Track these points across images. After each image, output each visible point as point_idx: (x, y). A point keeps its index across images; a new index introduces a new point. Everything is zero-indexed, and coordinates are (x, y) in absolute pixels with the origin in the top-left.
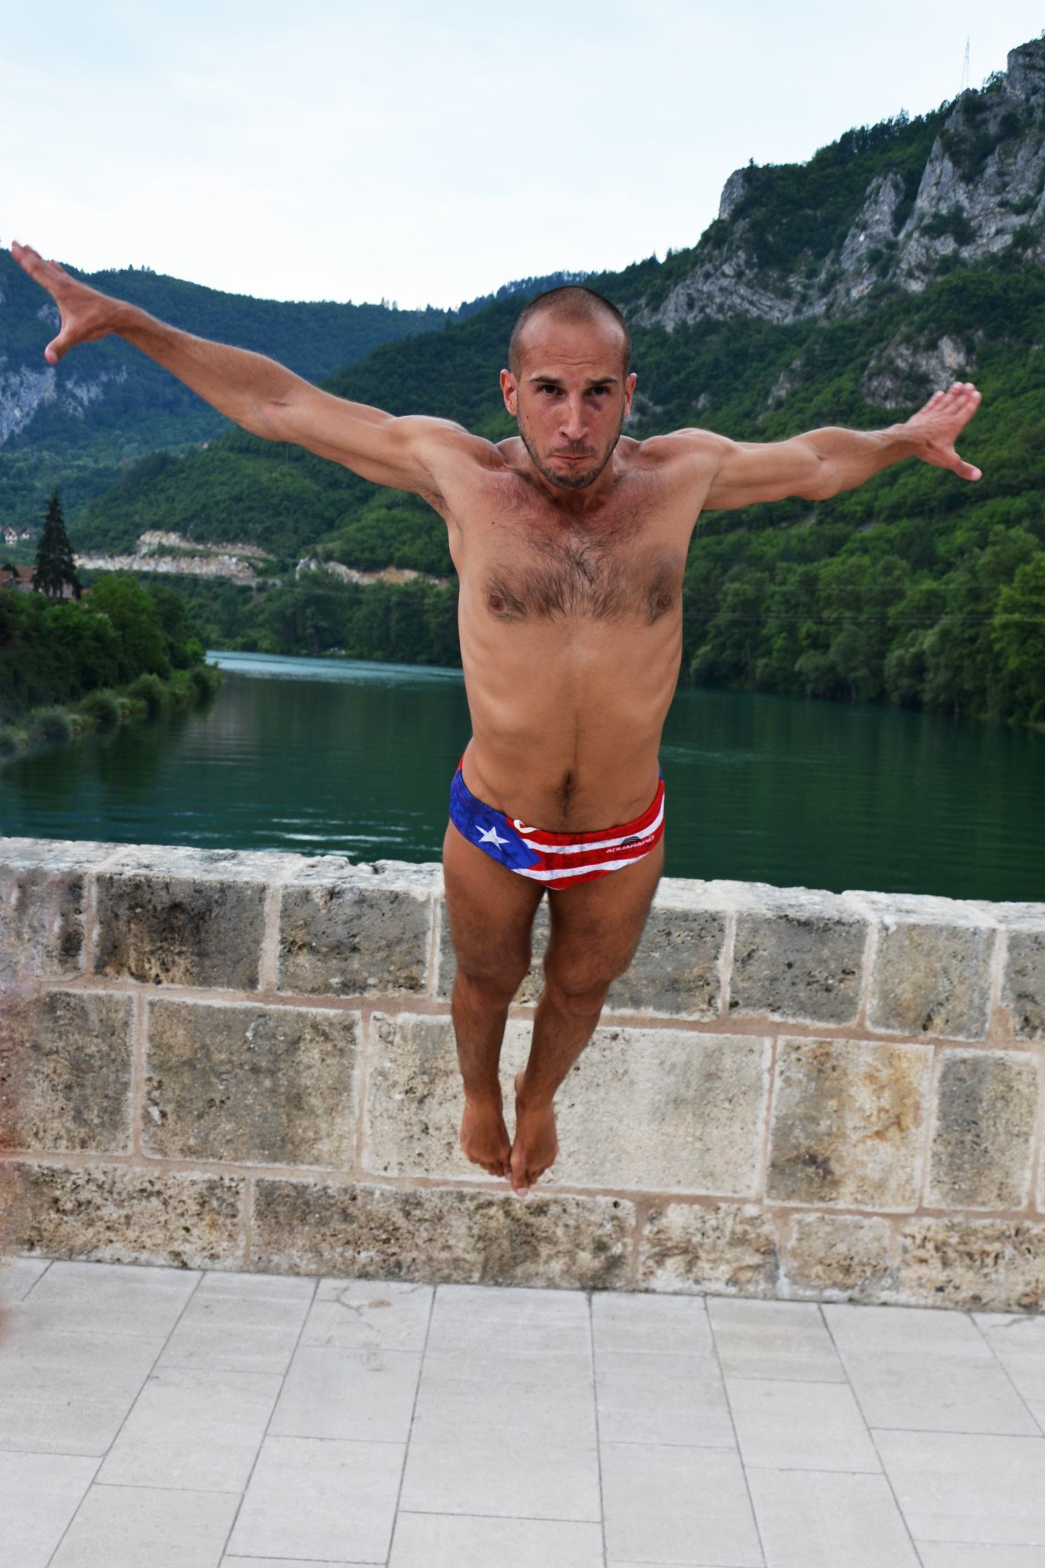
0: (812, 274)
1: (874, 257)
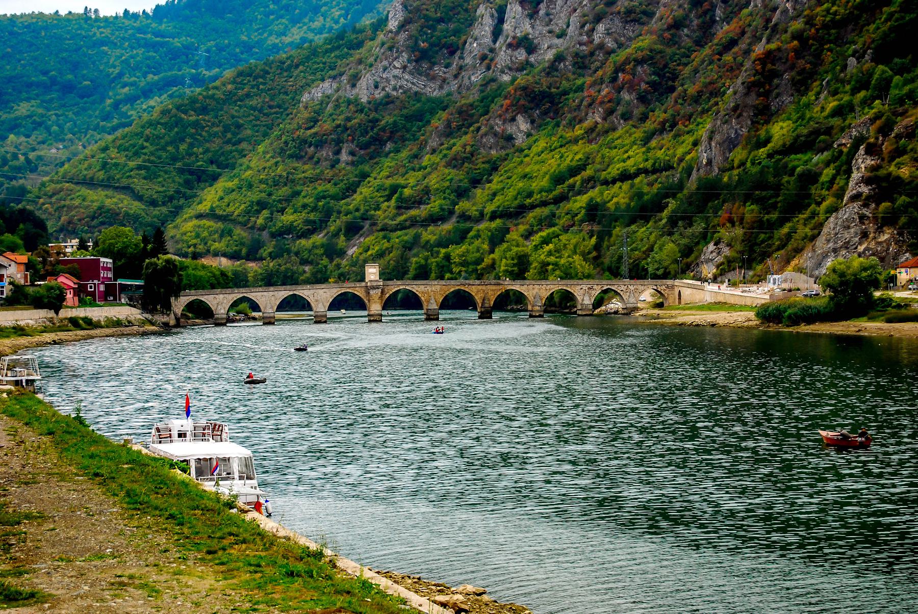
1: (483, 58)
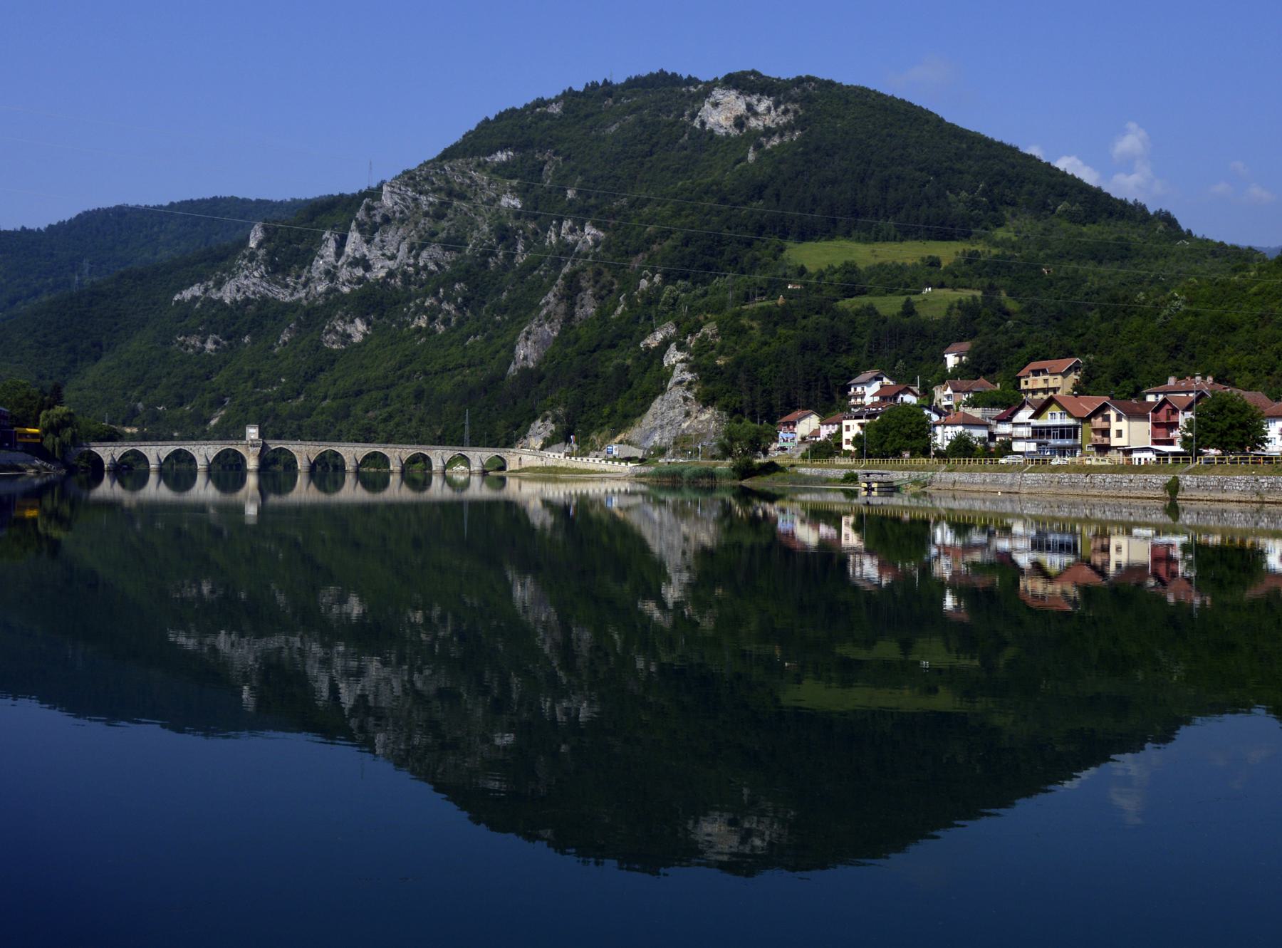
0: (299, 277)
1: (327, 272)
